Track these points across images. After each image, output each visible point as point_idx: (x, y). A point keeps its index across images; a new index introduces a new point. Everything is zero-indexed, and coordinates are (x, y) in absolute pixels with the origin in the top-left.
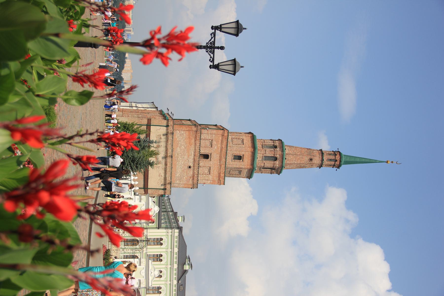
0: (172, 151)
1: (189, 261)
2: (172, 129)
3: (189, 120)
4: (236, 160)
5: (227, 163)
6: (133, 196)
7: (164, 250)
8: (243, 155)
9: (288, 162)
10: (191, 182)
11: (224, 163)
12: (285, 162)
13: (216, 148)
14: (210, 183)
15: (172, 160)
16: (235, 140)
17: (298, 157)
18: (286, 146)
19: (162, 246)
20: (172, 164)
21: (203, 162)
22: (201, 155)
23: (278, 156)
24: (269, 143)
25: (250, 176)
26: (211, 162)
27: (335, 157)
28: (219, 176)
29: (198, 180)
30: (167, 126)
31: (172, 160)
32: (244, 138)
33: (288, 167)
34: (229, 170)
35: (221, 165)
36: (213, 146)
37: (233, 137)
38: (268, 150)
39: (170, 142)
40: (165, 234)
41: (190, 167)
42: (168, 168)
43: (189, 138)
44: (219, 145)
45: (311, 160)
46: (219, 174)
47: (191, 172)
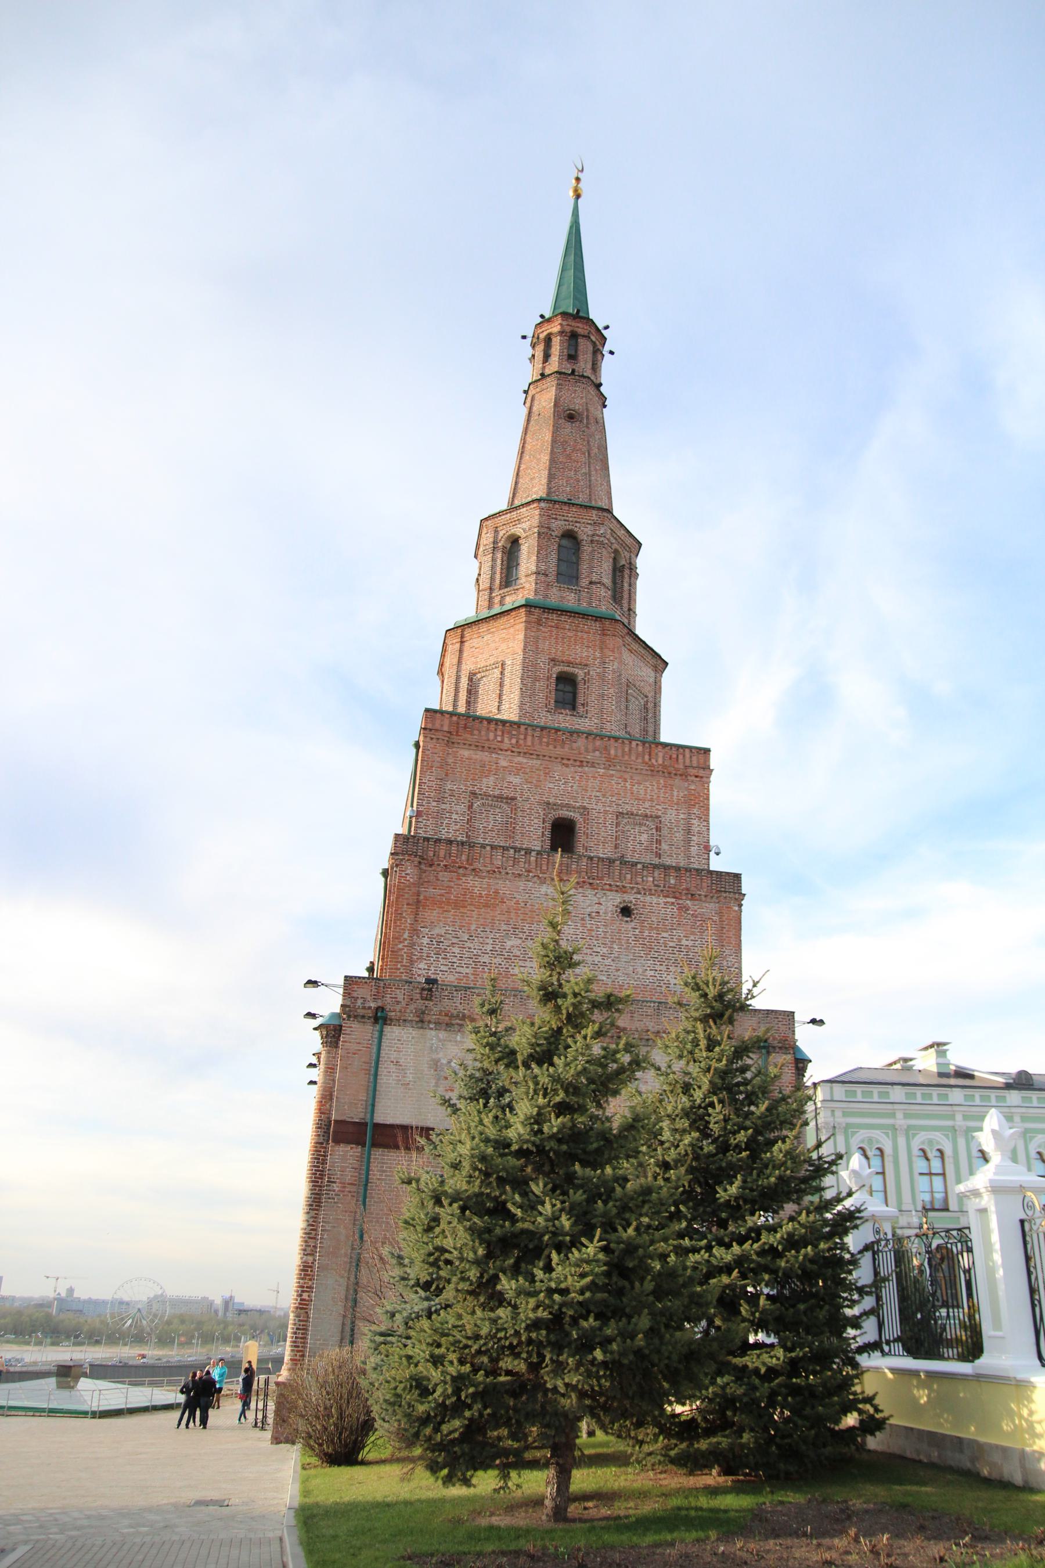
4: (580, 699)
7: (901, 1141)
10: (709, 908)
11: (598, 743)
12: (582, 499)
13: (516, 780)
14: (705, 817)
19: (888, 1150)
23: (558, 526)
30: (380, 1018)
32: (467, 667)
35: (610, 762)
36: (506, 792)
41: (626, 911)
43: (458, 905)
45: (571, 417)
46: (653, 772)
47: (656, 906)
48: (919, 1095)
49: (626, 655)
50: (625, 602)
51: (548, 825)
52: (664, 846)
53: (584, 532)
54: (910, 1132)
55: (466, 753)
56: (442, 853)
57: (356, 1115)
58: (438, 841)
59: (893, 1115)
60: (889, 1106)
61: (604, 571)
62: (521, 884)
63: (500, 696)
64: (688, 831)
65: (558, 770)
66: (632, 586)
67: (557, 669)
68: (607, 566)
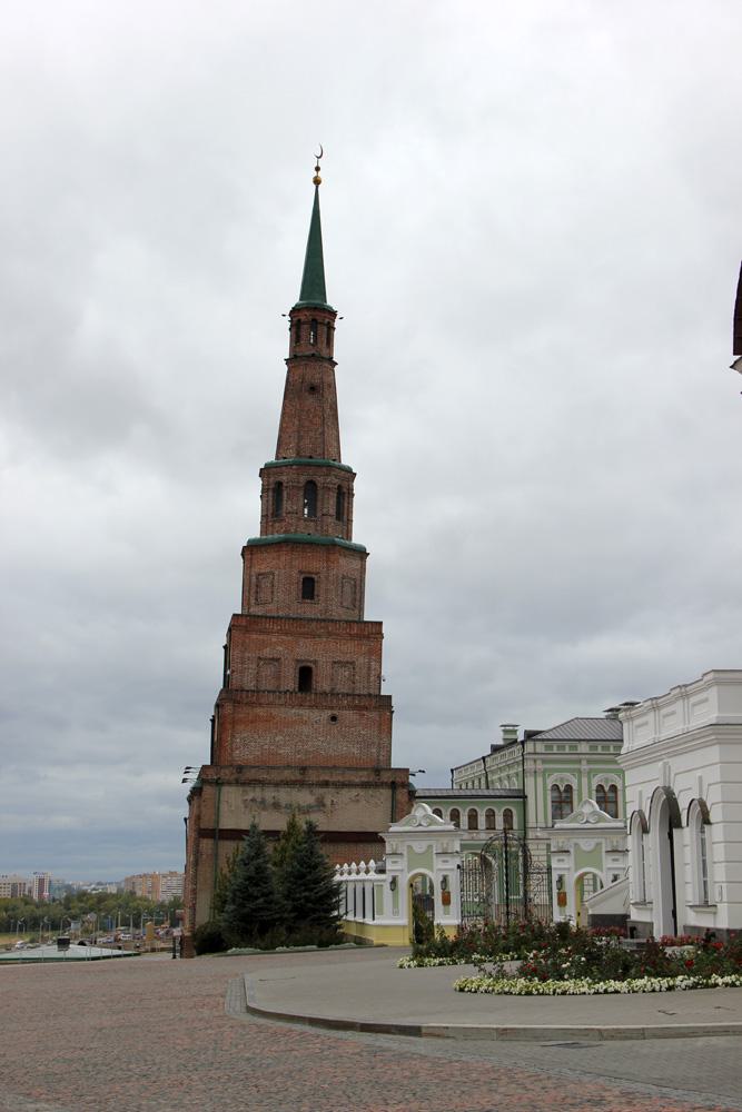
0: (288, 767)
1: (618, 710)
2: (227, 771)
3: (213, 721)
4: (316, 593)
5: (323, 617)
6: (387, 877)
7: (585, 780)
8: (301, 572)
9: (319, 451)
10: (374, 715)
11: (323, 624)
15: (316, 768)
16: (262, 595)
17: (307, 423)
18: (277, 458)
20: (324, 768)
21: (322, 683)
22: (301, 689)
23: (303, 479)
24: (271, 503)
25: (361, 553)
26: (322, 660)
27: (305, 323)
28: (360, 637)
29: (370, 695)
30: (218, 783)
31: (316, 768)
32: (256, 570)
33: (333, 451)
34: (341, 611)
35: (329, 634)
37: (253, 601)
38: (287, 505)
39: (263, 776)
40: (540, 780)
41: (334, 718)
42: (335, 779)
43: (252, 722)
44: (274, 640)
45: (313, 389)
48: (600, 748)
49: (343, 561)
50: (345, 516)
51: (297, 671)
52: (357, 677)
53: (320, 480)
54: (591, 773)
55: (255, 636)
56: (244, 696)
57: (211, 826)
58: (242, 690)
59: (579, 761)
60: (576, 756)
61: (330, 505)
62: (282, 709)
63: (272, 592)
64: (369, 669)
65: (302, 641)
66: (350, 503)
67: (303, 576)
68: (332, 502)
